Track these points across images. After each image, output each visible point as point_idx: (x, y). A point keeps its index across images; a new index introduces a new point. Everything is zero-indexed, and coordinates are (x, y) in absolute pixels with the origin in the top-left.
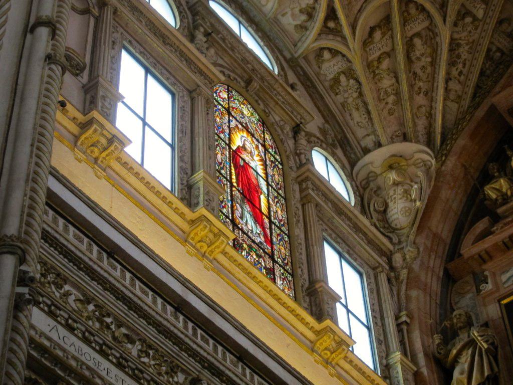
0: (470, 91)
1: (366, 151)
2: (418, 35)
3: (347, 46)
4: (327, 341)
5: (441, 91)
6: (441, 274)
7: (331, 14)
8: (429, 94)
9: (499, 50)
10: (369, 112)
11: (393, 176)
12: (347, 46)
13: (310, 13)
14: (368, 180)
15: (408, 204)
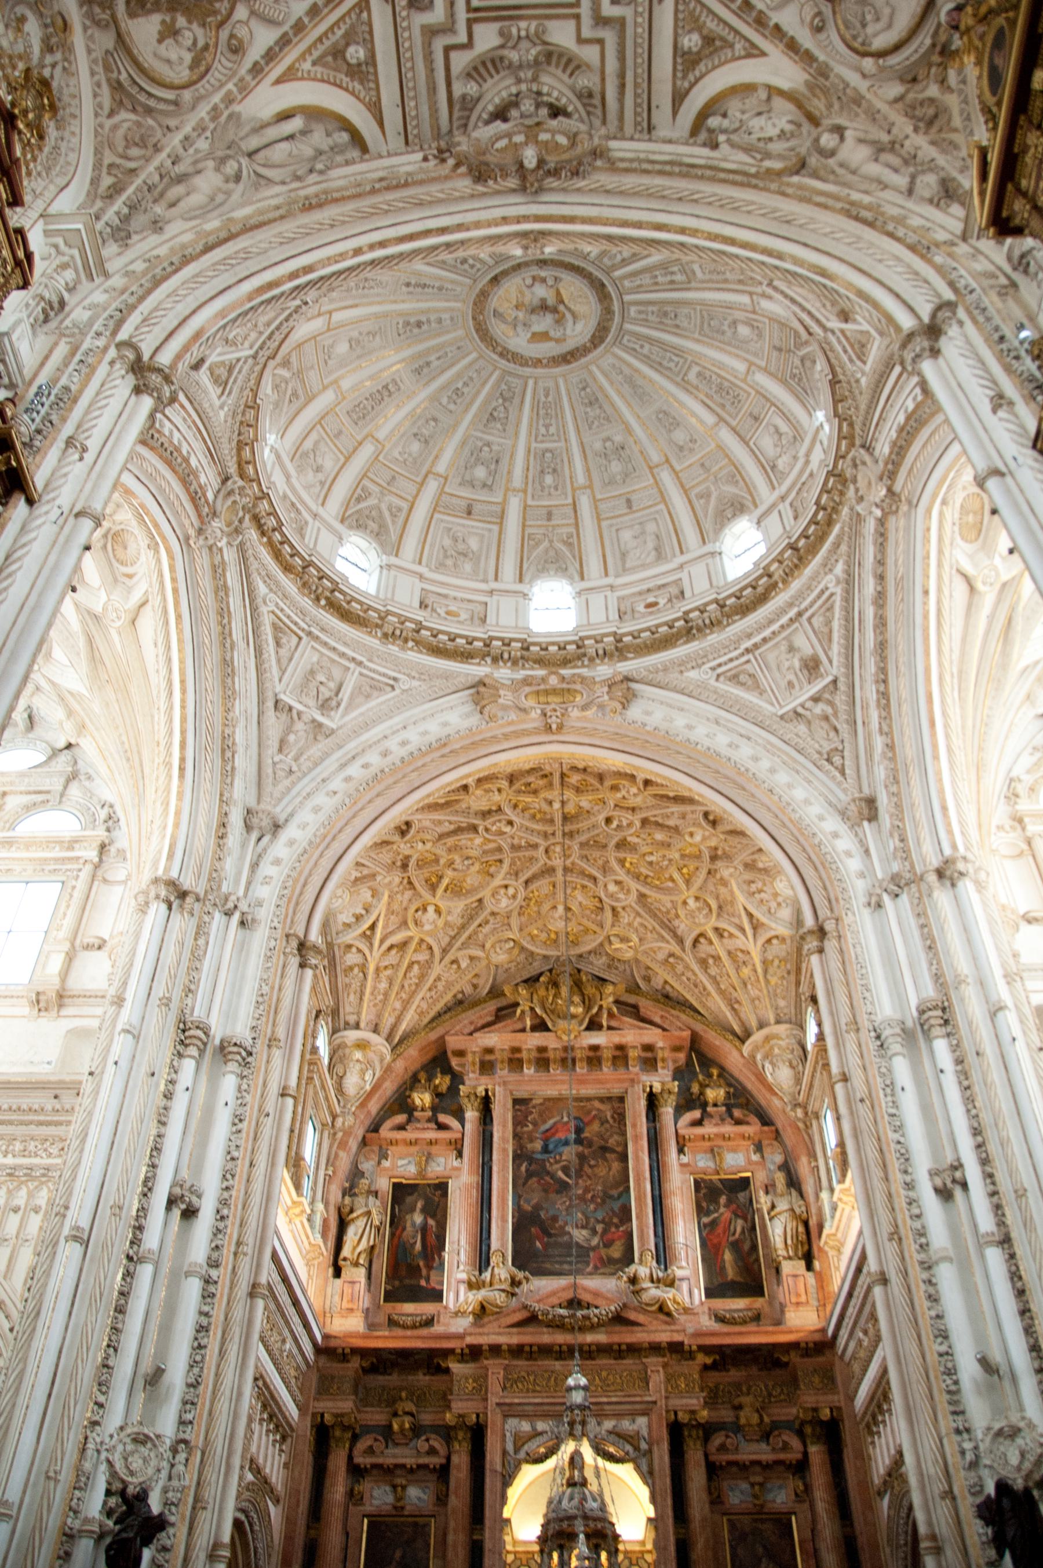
0: (432, 1014)
1: (347, 1026)
2: (418, 962)
3: (371, 951)
4: (297, 1211)
5: (414, 1007)
6: (360, 1138)
7: (373, 927)
8: (406, 1004)
9: (462, 992)
10: (361, 999)
11: (358, 1055)
12: (371, 951)
13: (358, 918)
14: (339, 1046)
15: (360, 1081)
